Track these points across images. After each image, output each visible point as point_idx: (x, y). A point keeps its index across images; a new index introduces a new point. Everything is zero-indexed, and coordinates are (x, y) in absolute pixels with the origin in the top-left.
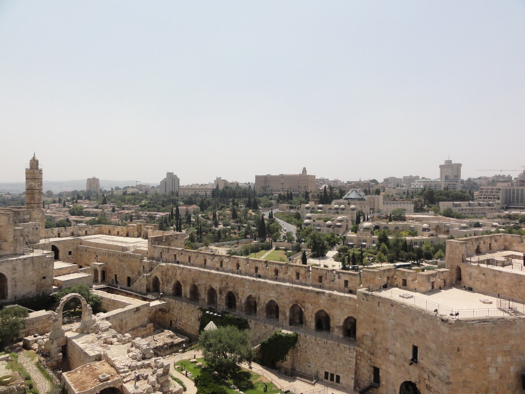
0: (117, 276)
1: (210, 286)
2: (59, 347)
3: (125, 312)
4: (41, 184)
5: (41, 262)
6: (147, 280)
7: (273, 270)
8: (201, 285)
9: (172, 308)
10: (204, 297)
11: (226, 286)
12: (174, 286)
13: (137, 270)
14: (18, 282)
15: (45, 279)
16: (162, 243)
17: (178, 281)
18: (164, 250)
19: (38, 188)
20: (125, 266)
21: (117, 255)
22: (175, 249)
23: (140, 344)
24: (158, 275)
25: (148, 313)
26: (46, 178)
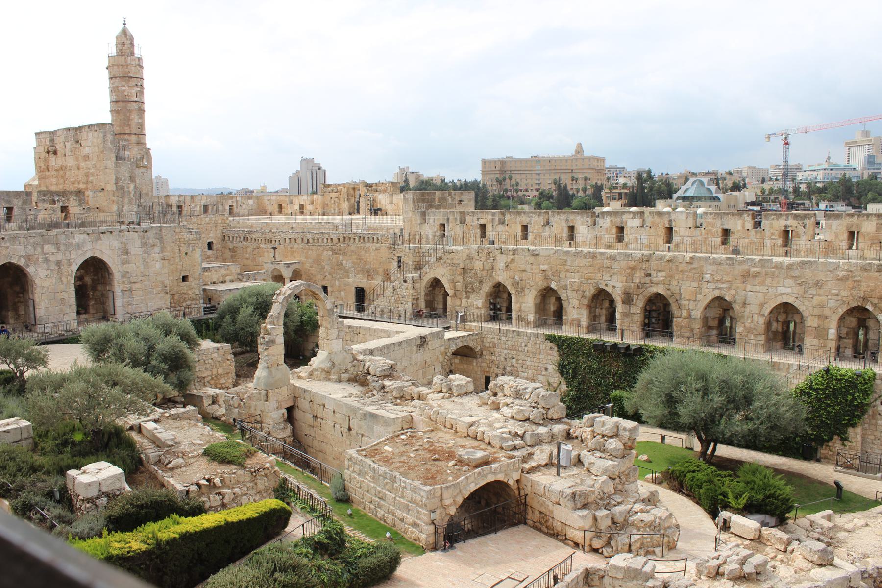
2: (281, 409)
3: (401, 343)
4: (141, 92)
5: (176, 240)
7: (776, 233)
8: (569, 287)
9: (491, 345)
10: (576, 316)
11: (642, 281)
12: (487, 296)
13: (381, 270)
18: (451, 217)
19: (136, 99)
20: (347, 263)
21: (325, 241)
23: (524, 387)
24: (442, 273)
25: (441, 354)
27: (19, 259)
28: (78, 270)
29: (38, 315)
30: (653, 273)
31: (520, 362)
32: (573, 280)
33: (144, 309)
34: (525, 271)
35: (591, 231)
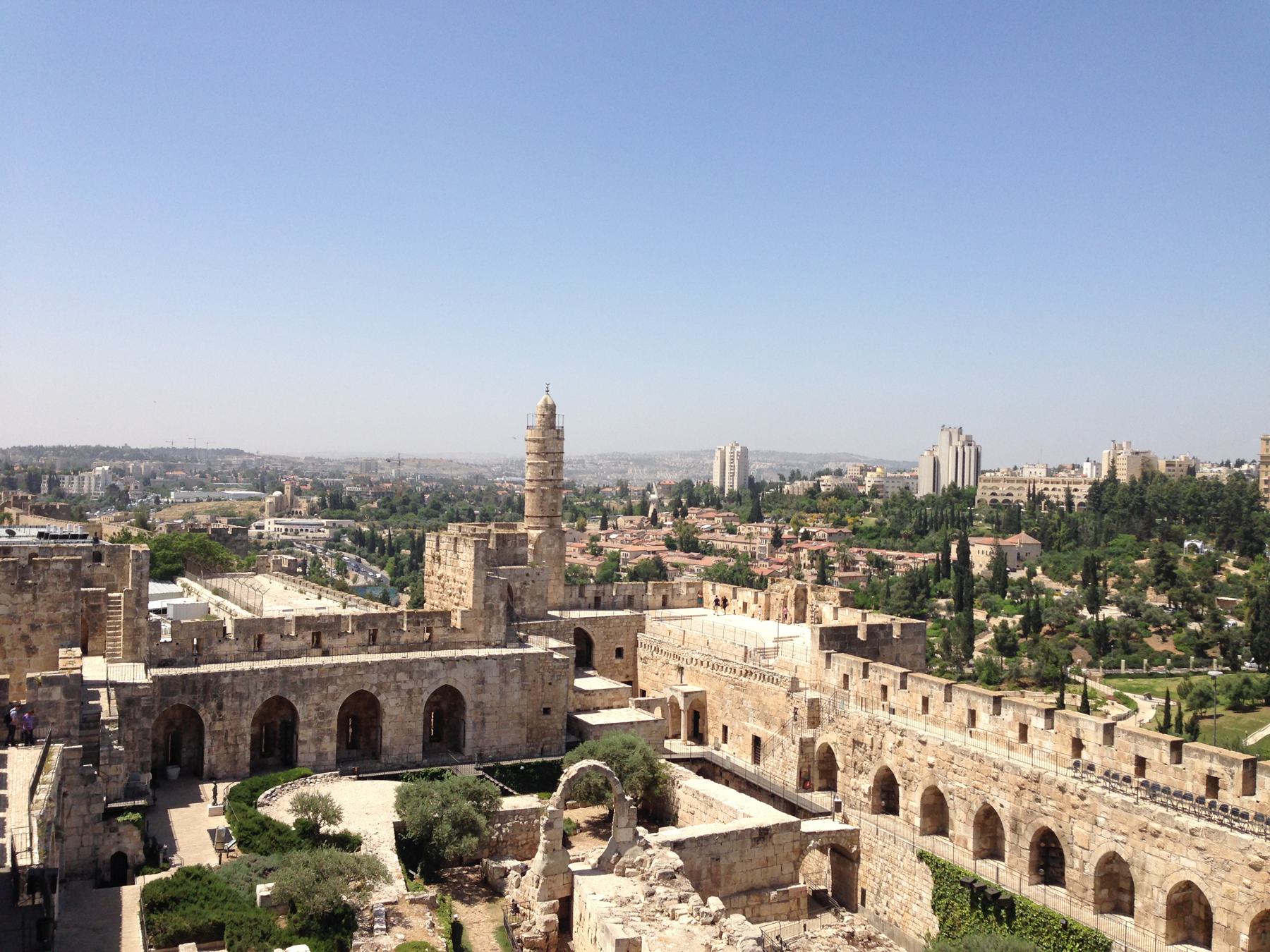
0: (729, 731)
1: (985, 803)
3: (726, 836)
4: (559, 468)
6: (802, 752)
7: (1199, 777)
8: (955, 793)
10: (963, 833)
11: (1032, 806)
12: (876, 781)
14: (488, 714)
15: (548, 717)
16: (854, 648)
17: (888, 769)
18: (855, 668)
19: (552, 477)
20: (748, 704)
22: (884, 669)
25: (794, 851)
26: (571, 449)
27: (371, 688)
28: (435, 693)
29: (383, 745)
30: (1042, 798)
31: (896, 879)
32: (960, 785)
33: (496, 743)
34: (912, 760)
35: (993, 721)
